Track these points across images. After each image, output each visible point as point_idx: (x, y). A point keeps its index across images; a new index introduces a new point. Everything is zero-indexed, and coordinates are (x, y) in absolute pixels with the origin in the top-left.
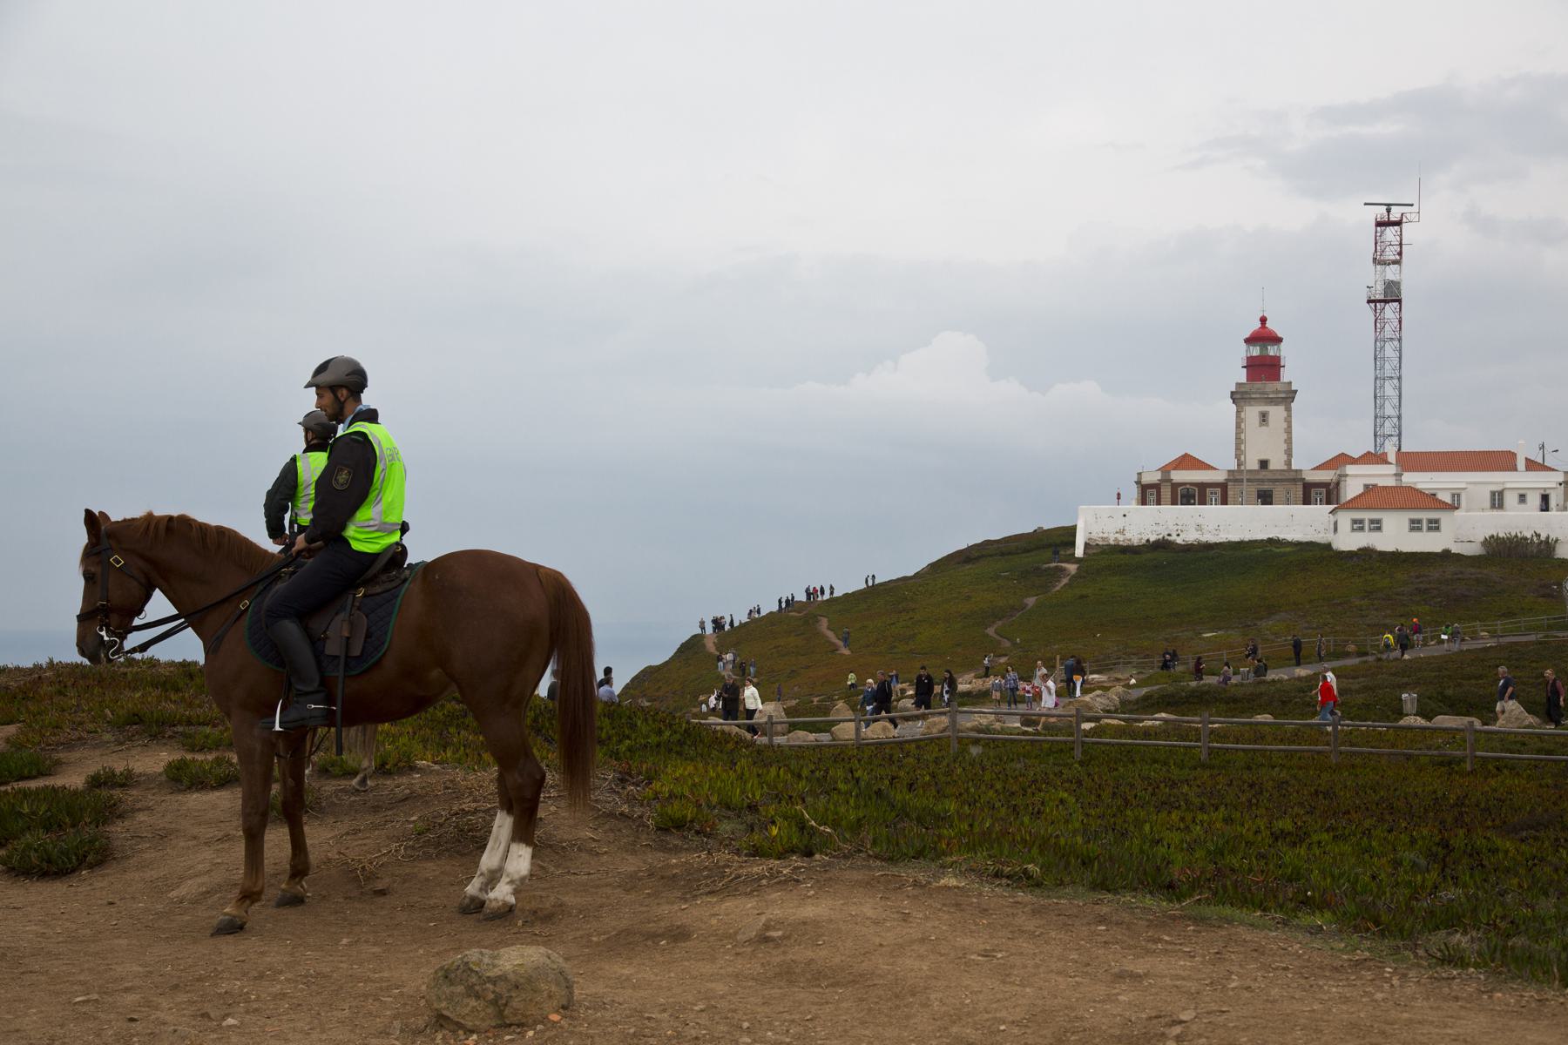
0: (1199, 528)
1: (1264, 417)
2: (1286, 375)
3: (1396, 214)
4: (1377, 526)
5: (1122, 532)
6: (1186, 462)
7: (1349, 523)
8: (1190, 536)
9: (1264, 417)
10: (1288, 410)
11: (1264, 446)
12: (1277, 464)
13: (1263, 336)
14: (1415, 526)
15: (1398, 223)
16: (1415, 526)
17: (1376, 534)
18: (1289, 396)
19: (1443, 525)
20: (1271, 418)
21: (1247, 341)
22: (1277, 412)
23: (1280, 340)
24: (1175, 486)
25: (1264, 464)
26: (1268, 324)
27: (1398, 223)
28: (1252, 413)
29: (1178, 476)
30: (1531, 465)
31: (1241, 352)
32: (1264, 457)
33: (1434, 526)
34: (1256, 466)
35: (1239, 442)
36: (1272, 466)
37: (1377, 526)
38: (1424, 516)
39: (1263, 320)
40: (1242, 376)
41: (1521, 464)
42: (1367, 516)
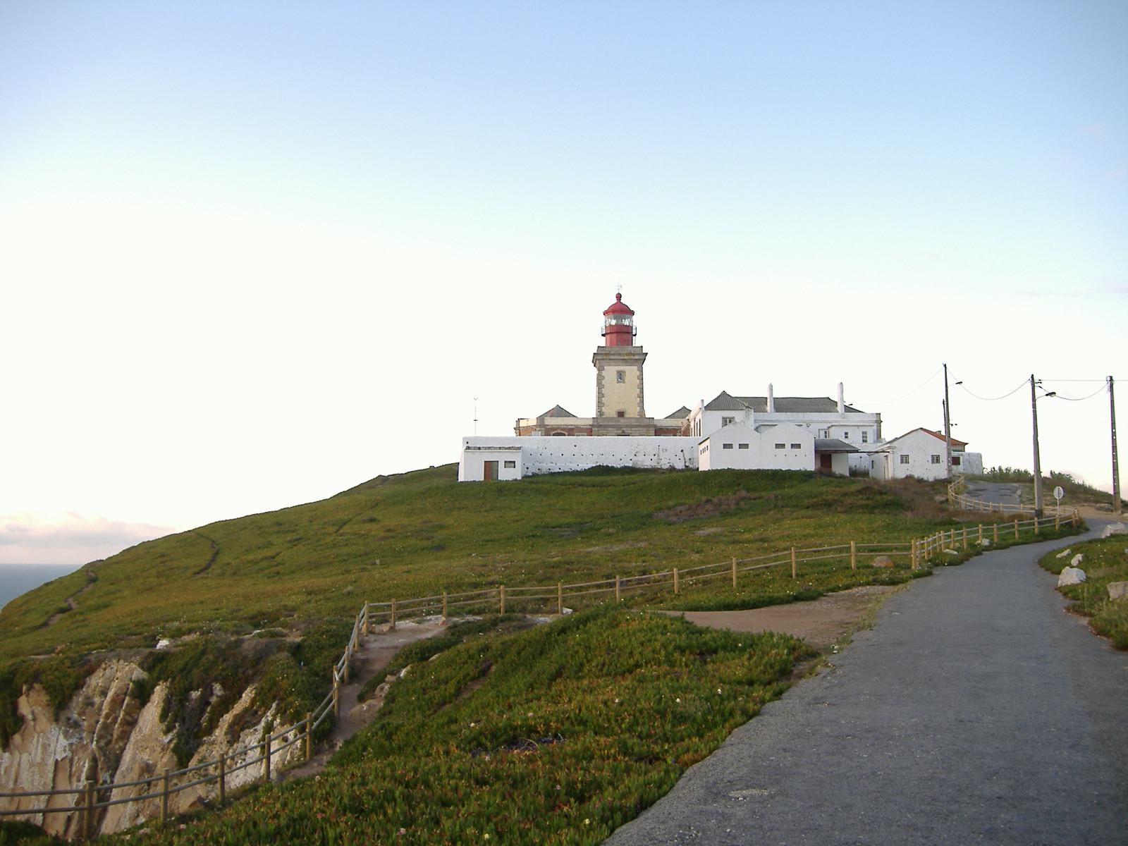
1: (621, 376)
2: (637, 342)
6: (559, 412)
9: (621, 376)
10: (641, 371)
11: (619, 398)
12: (632, 412)
13: (620, 310)
18: (640, 358)
21: (605, 313)
22: (631, 370)
23: (632, 313)
28: (611, 371)
29: (550, 421)
31: (601, 322)
32: (620, 408)
34: (615, 416)
35: (600, 395)
36: (627, 416)
39: (619, 297)
40: (602, 342)
41: (840, 408)
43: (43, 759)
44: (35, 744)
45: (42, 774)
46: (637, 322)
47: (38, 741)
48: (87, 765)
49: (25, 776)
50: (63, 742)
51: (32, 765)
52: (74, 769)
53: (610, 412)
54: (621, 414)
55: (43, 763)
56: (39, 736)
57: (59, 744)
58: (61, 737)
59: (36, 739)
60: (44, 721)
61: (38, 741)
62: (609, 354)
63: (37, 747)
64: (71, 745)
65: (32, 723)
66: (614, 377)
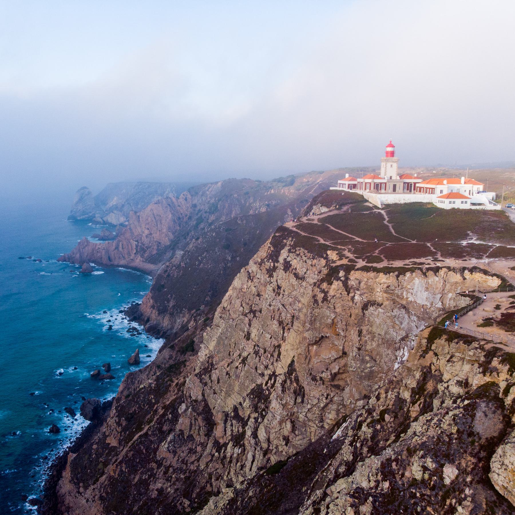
0: (404, 199)
4: (454, 203)
5: (387, 200)
8: (402, 202)
14: (462, 202)
24: (375, 183)
25: (391, 178)
28: (389, 164)
30: (465, 183)
33: (466, 203)
36: (393, 178)
37: (454, 203)
38: (464, 200)
39: (391, 142)
42: (452, 200)
46: (395, 149)
49: (430, 283)
55: (434, 281)
57: (437, 279)
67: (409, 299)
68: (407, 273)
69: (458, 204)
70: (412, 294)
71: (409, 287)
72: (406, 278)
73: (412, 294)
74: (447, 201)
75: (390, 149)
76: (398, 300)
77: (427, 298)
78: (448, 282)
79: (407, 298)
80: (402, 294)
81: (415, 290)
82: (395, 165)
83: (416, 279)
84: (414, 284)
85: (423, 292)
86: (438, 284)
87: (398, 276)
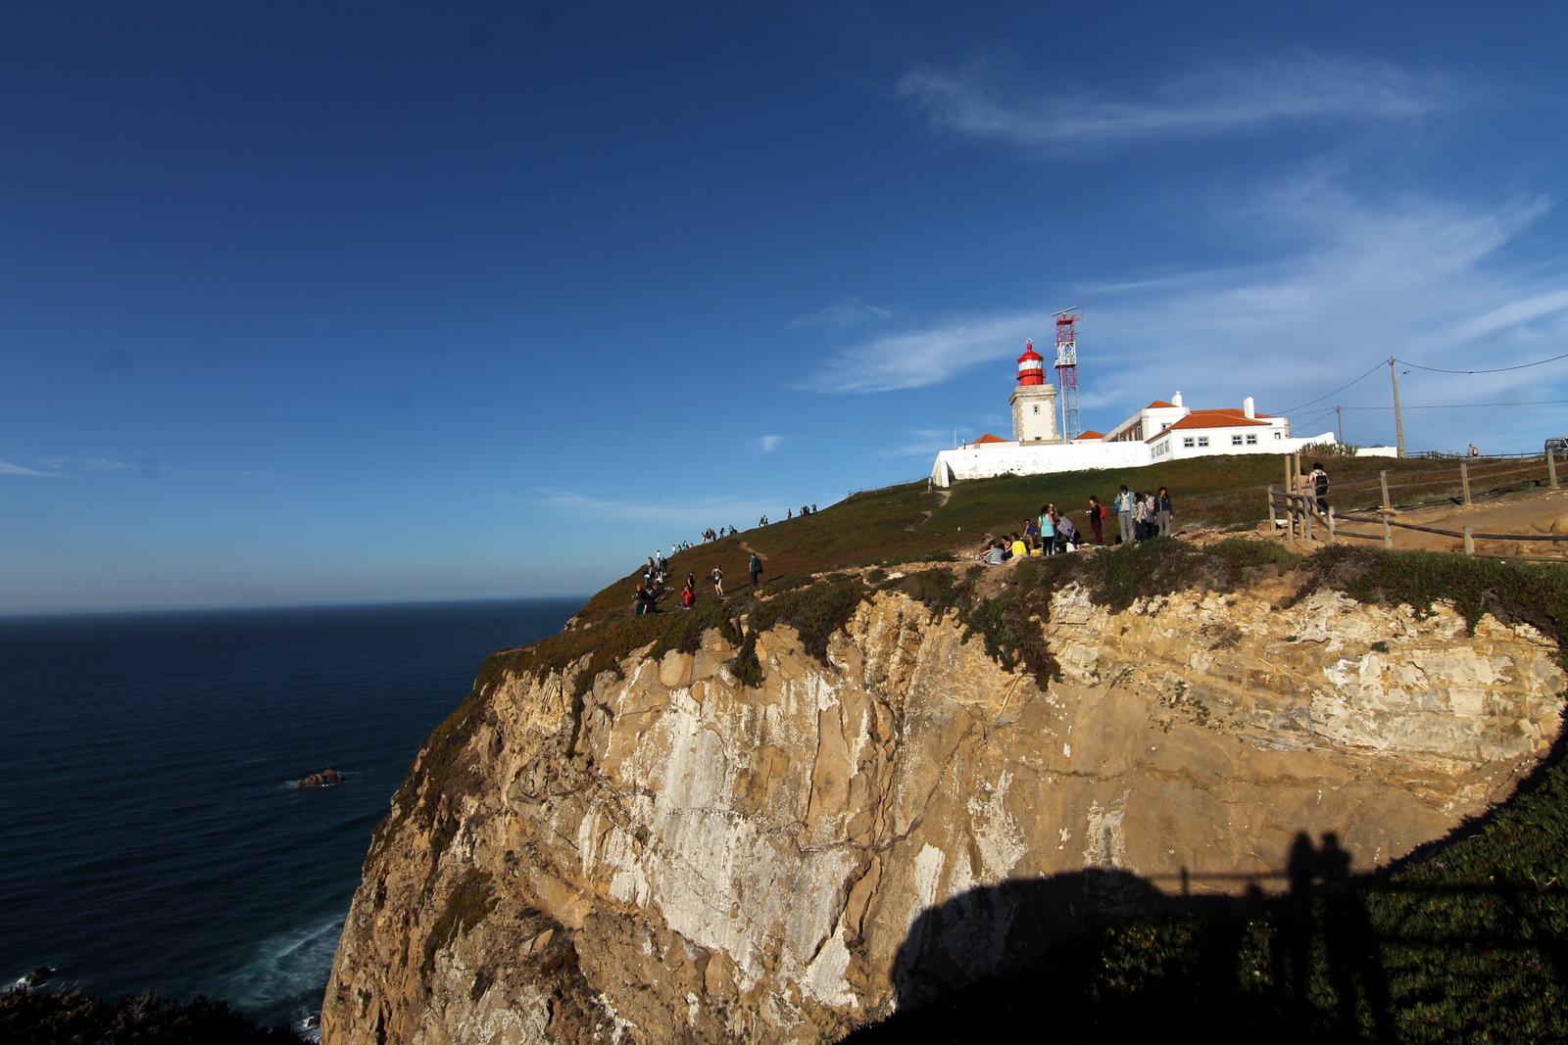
3: (1068, 319)
4: (1204, 443)
5: (975, 469)
7: (1182, 443)
9: (1036, 410)
14: (1237, 441)
15: (1070, 322)
16: (1237, 441)
17: (1204, 448)
19: (1259, 439)
20: (1040, 409)
26: (1034, 350)
27: (1070, 322)
32: (1038, 436)
33: (1252, 440)
34: (1033, 439)
36: (1043, 439)
38: (1243, 431)
42: (1196, 434)
43: (799, 711)
44: (785, 693)
45: (802, 727)
47: (789, 690)
48: (865, 714)
49: (776, 731)
50: (825, 687)
51: (783, 717)
52: (846, 720)
53: (1029, 436)
54: (1038, 439)
56: (789, 684)
57: (822, 693)
58: (822, 682)
59: (784, 687)
60: (792, 662)
61: (789, 690)
62: (1024, 392)
63: (788, 698)
64: (837, 691)
65: (776, 669)
66: (1033, 410)
67: (619, 888)
68: (636, 655)
69: (1220, 442)
70: (641, 836)
71: (627, 774)
72: (624, 694)
73: (641, 836)
74: (1177, 437)
75: (1029, 365)
76: (546, 890)
77: (737, 885)
78: (916, 722)
79: (603, 873)
80: (568, 833)
81: (667, 799)
82: (1046, 407)
83: (682, 697)
84: (664, 745)
85: (716, 820)
86: (832, 739)
87: (584, 683)
